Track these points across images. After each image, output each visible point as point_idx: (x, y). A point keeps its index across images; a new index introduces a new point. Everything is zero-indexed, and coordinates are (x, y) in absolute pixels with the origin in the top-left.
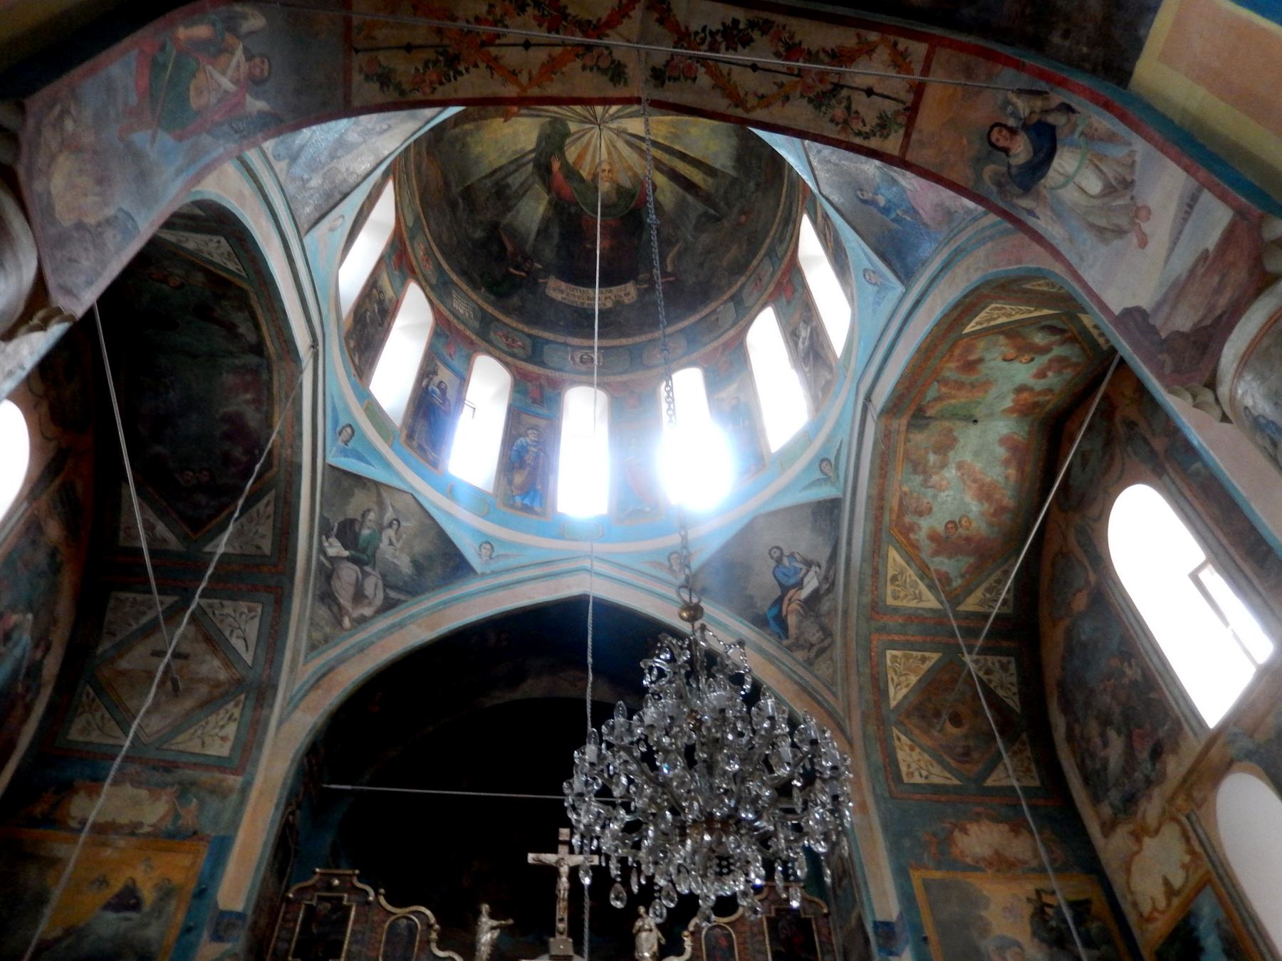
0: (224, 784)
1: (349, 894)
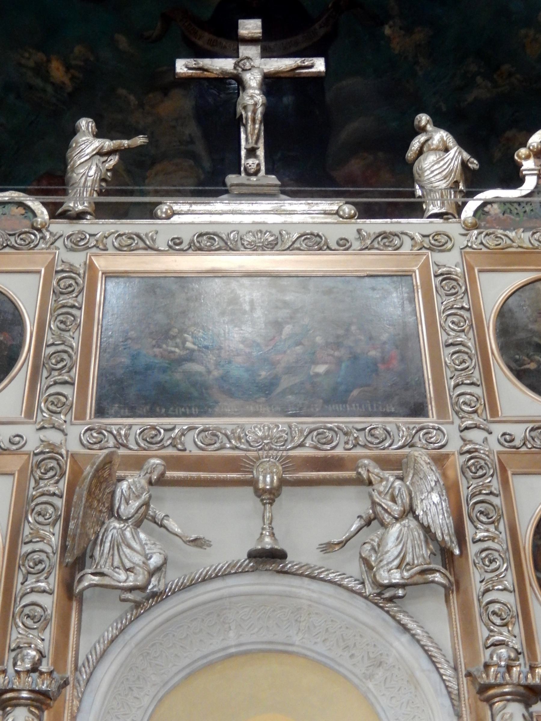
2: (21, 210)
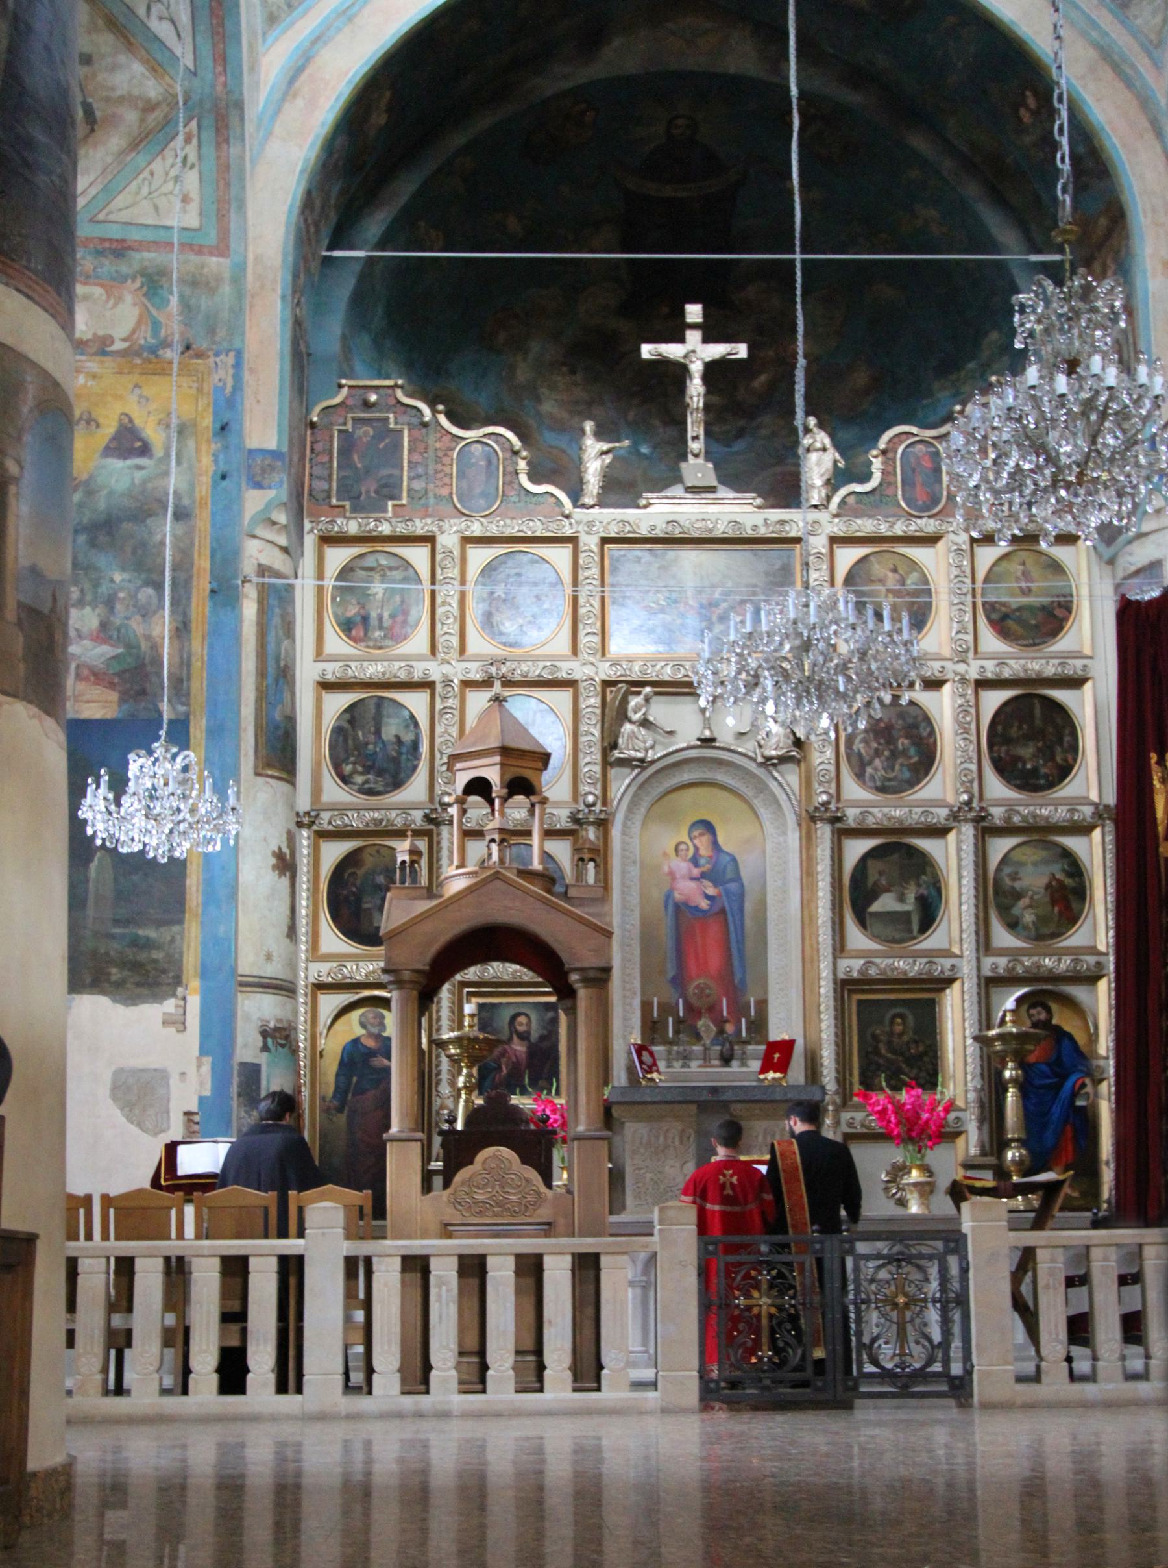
1: (395, 413)
2: (553, 500)
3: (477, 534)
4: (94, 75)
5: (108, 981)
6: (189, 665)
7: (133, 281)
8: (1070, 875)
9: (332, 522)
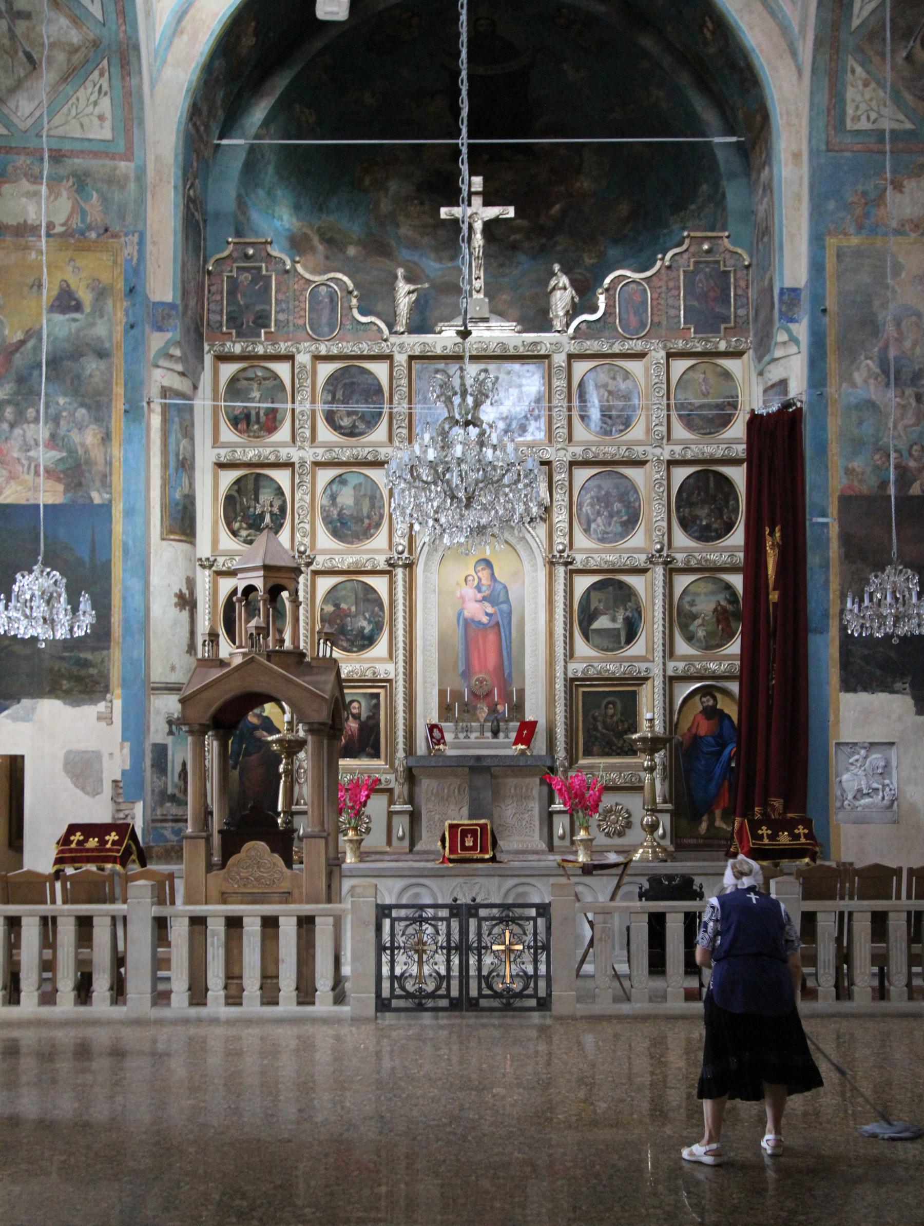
0: (118, 172)
3: (323, 353)
4: (34, 27)
5: (60, 689)
6: (111, 464)
7: (67, 181)
8: (730, 602)
9: (223, 345)
